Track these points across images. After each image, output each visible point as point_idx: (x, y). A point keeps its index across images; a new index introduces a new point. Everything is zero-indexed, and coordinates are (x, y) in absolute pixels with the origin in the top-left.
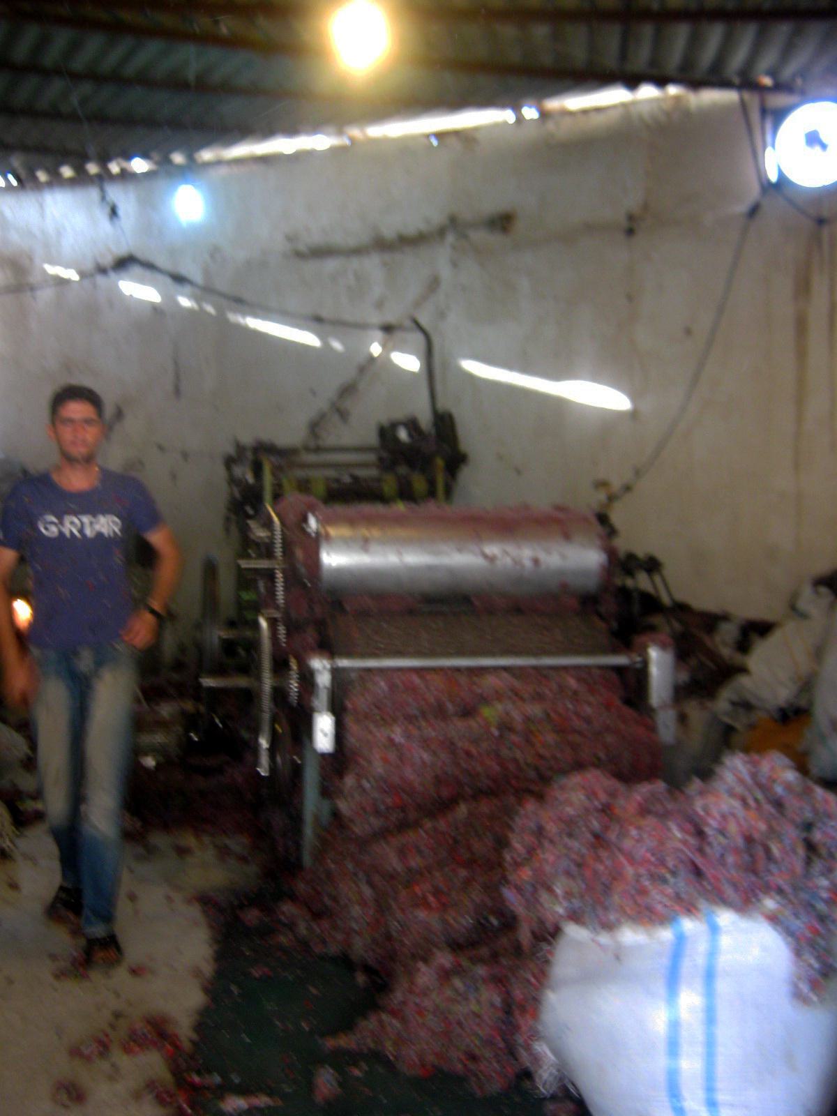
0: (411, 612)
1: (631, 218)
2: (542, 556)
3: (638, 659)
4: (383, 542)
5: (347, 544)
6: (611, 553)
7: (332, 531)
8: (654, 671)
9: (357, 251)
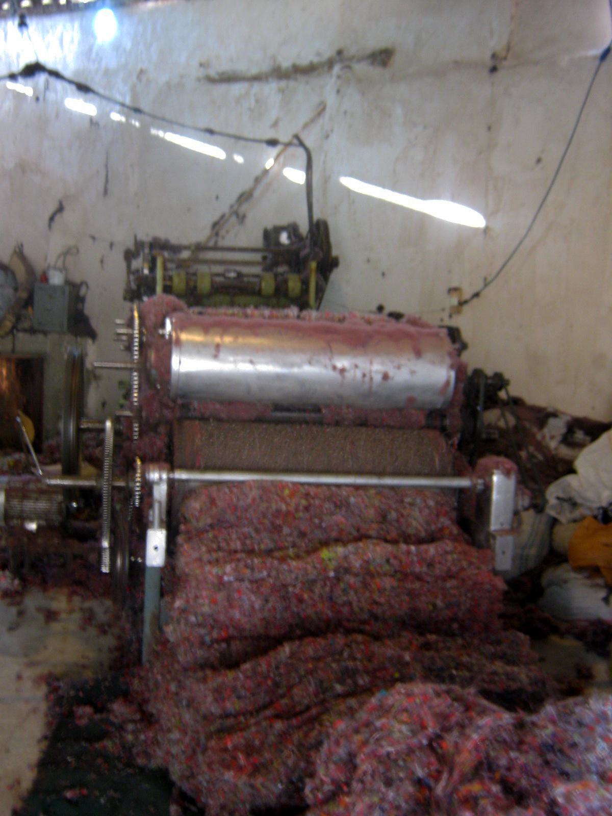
0: (259, 420)
1: (494, 56)
2: (392, 372)
3: (480, 481)
4: (235, 350)
5: (198, 349)
6: (460, 370)
7: (184, 336)
8: (495, 496)
9: (257, 78)
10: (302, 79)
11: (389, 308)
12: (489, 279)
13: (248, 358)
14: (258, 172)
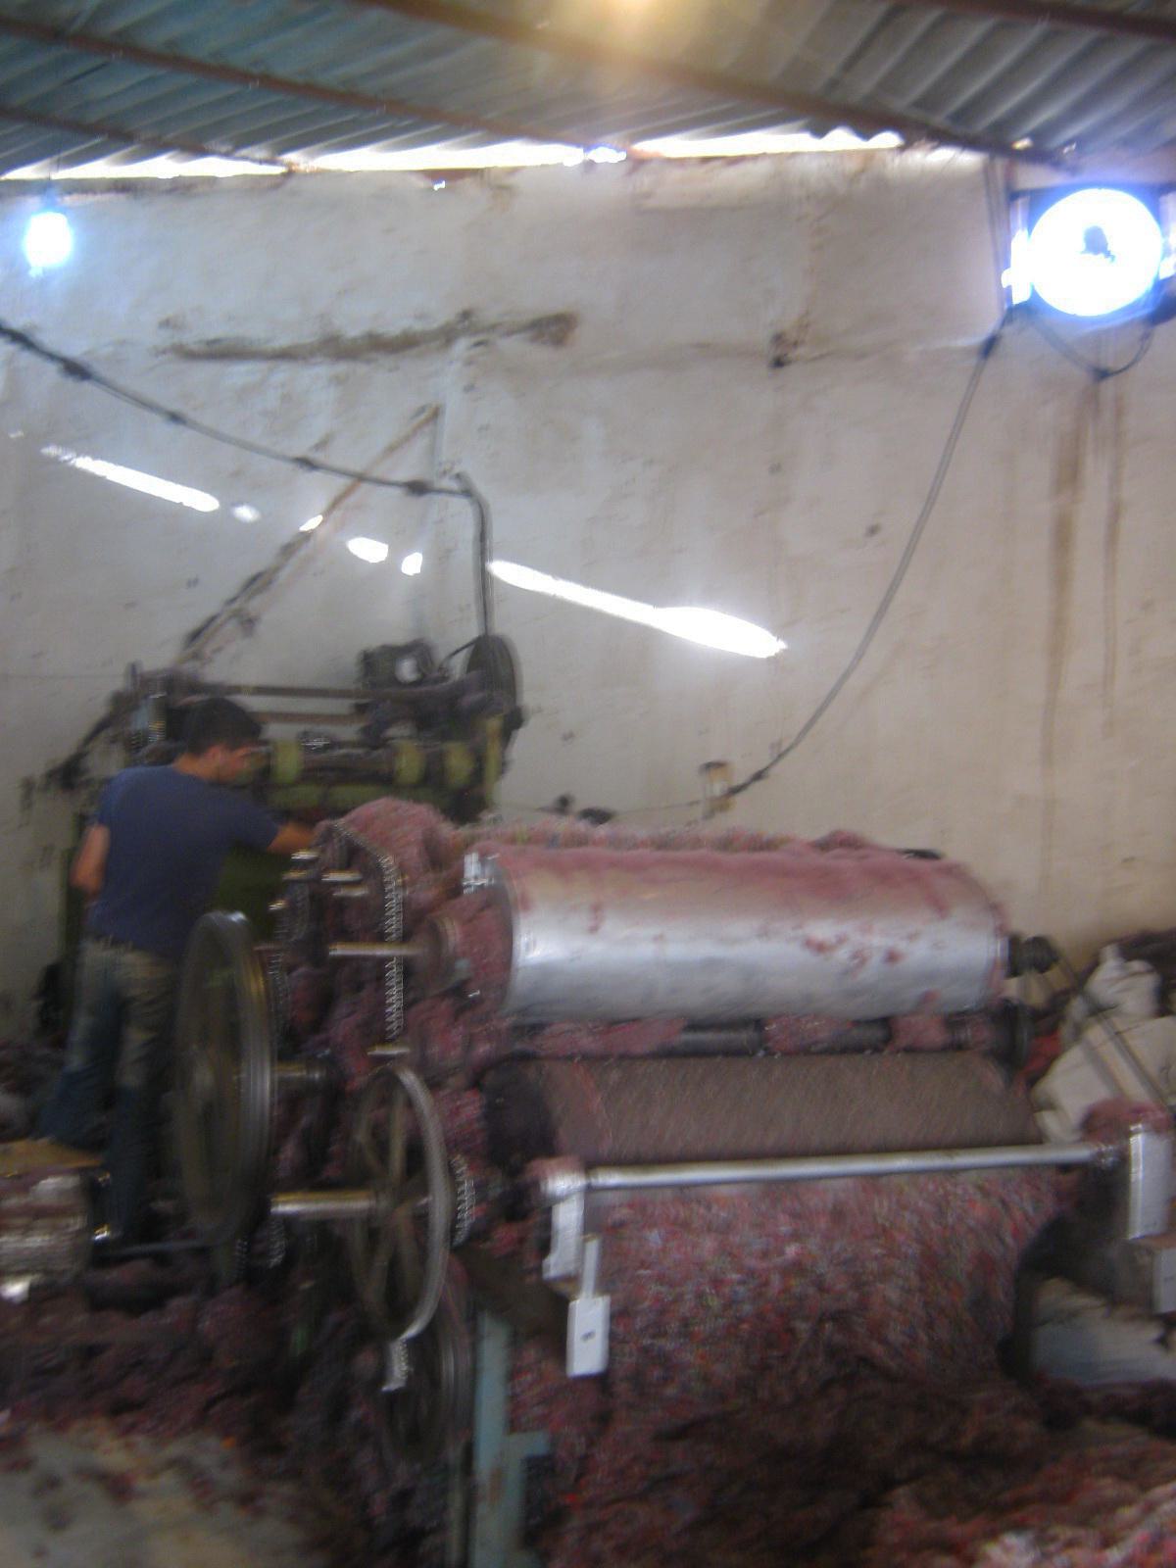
1: (778, 339)
2: (902, 946)
10: (386, 361)
11: (582, 803)
13: (654, 931)
14: (285, 537)
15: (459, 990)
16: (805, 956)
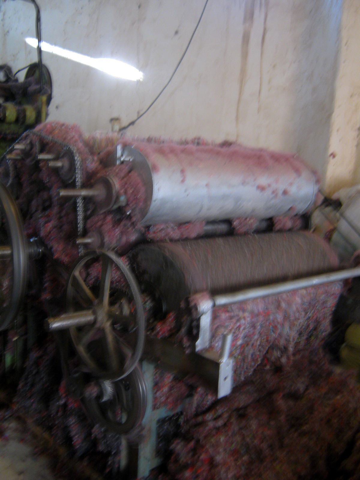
12: (141, 113)
15: (120, 210)
16: (258, 193)
